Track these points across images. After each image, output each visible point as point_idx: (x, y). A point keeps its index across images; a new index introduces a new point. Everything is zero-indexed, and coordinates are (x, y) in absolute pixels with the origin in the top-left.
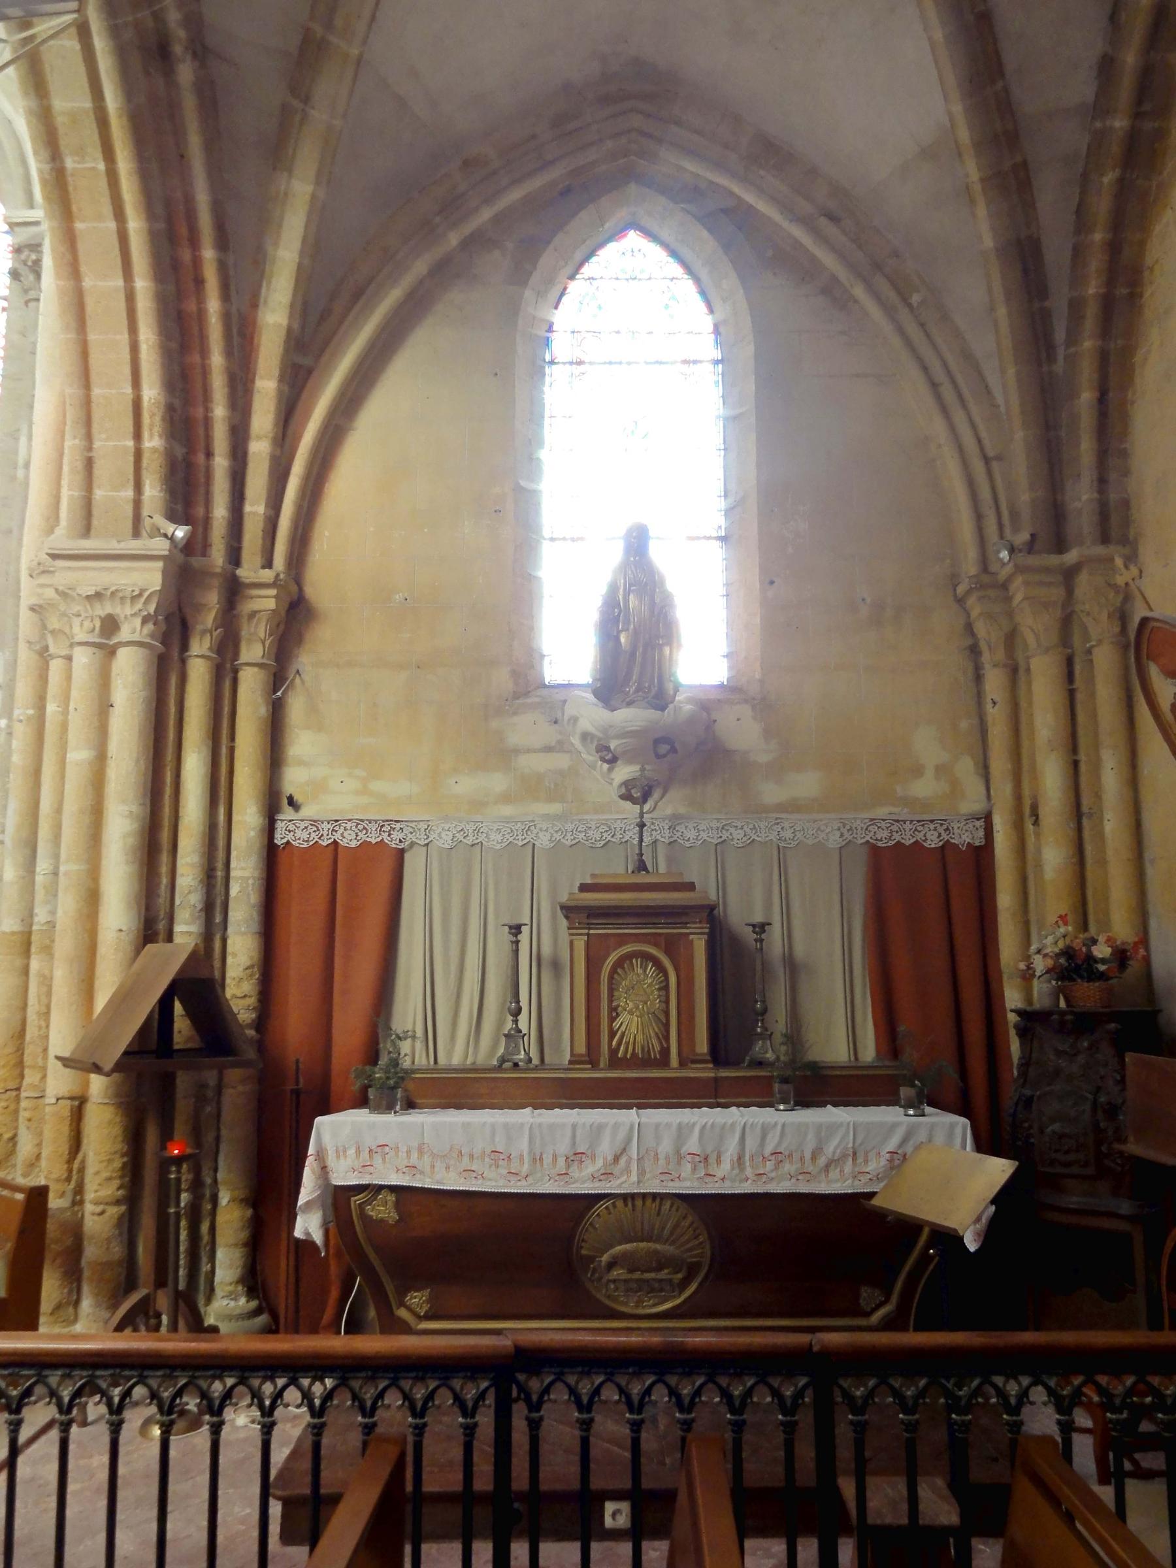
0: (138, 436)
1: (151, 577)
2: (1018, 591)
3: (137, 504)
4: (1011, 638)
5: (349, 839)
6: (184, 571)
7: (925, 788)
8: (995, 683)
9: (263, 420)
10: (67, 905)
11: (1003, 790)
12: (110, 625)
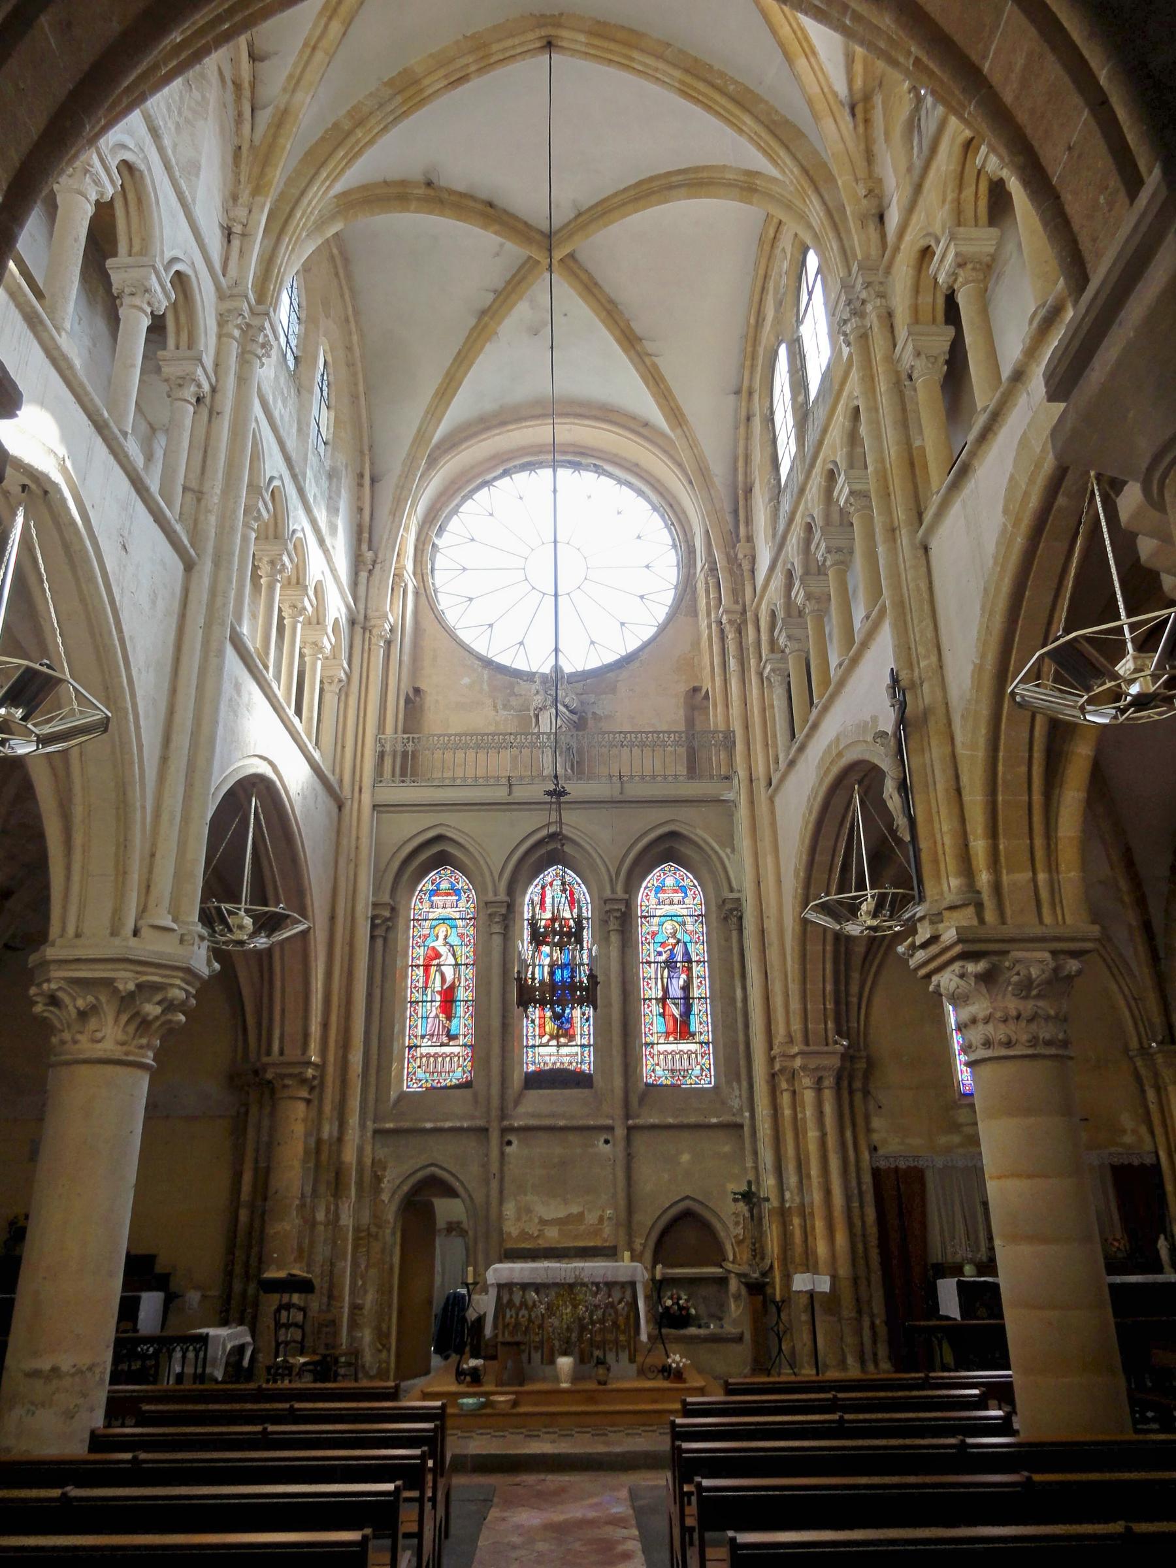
0: (824, 1004)
1: (835, 1062)
2: (1159, 1059)
3: (826, 1030)
4: (1156, 1075)
5: (902, 1165)
6: (848, 1057)
7: (1128, 1139)
8: (1151, 1095)
9: (854, 989)
10: (817, 1197)
11: (1161, 1139)
12: (820, 1080)
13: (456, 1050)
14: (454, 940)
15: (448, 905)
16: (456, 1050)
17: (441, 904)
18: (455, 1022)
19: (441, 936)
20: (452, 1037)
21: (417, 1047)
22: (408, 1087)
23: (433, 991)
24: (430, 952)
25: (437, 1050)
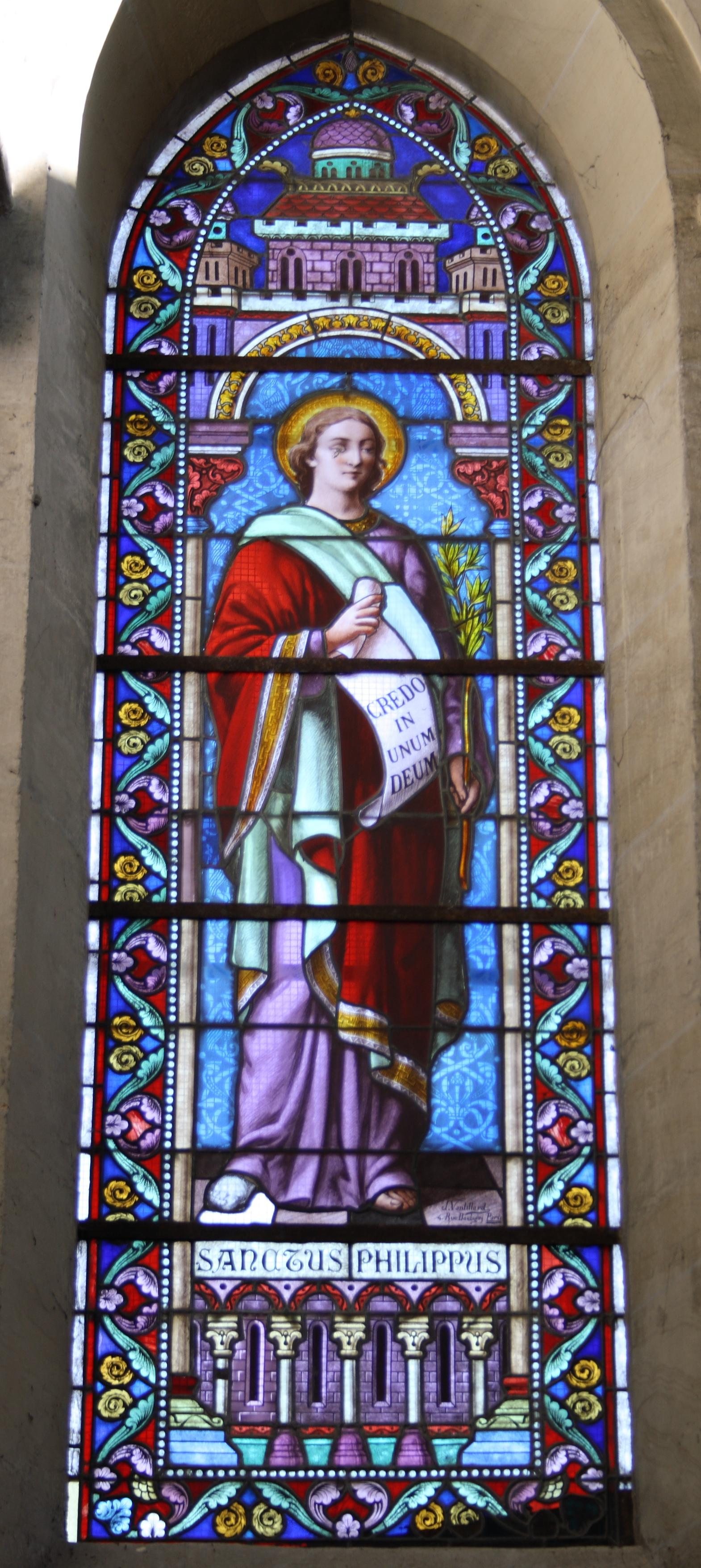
13: (479, 1264)
14: (425, 497)
15: (380, 269)
16: (479, 1264)
17: (321, 265)
18: (459, 1068)
19: (333, 473)
20: (445, 1178)
21: (162, 1232)
22: (87, 1520)
23: (280, 844)
24: (256, 580)
25: (325, 1259)
